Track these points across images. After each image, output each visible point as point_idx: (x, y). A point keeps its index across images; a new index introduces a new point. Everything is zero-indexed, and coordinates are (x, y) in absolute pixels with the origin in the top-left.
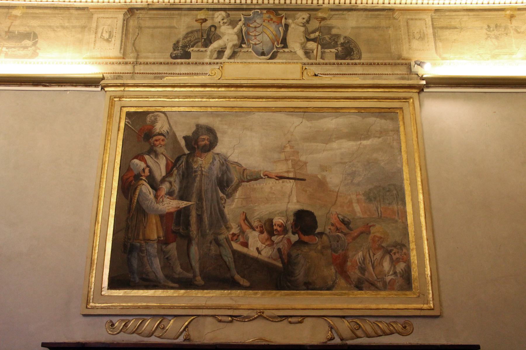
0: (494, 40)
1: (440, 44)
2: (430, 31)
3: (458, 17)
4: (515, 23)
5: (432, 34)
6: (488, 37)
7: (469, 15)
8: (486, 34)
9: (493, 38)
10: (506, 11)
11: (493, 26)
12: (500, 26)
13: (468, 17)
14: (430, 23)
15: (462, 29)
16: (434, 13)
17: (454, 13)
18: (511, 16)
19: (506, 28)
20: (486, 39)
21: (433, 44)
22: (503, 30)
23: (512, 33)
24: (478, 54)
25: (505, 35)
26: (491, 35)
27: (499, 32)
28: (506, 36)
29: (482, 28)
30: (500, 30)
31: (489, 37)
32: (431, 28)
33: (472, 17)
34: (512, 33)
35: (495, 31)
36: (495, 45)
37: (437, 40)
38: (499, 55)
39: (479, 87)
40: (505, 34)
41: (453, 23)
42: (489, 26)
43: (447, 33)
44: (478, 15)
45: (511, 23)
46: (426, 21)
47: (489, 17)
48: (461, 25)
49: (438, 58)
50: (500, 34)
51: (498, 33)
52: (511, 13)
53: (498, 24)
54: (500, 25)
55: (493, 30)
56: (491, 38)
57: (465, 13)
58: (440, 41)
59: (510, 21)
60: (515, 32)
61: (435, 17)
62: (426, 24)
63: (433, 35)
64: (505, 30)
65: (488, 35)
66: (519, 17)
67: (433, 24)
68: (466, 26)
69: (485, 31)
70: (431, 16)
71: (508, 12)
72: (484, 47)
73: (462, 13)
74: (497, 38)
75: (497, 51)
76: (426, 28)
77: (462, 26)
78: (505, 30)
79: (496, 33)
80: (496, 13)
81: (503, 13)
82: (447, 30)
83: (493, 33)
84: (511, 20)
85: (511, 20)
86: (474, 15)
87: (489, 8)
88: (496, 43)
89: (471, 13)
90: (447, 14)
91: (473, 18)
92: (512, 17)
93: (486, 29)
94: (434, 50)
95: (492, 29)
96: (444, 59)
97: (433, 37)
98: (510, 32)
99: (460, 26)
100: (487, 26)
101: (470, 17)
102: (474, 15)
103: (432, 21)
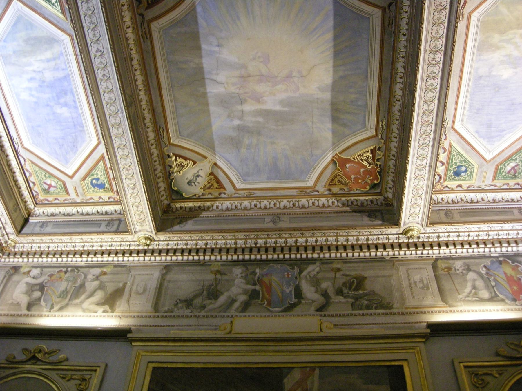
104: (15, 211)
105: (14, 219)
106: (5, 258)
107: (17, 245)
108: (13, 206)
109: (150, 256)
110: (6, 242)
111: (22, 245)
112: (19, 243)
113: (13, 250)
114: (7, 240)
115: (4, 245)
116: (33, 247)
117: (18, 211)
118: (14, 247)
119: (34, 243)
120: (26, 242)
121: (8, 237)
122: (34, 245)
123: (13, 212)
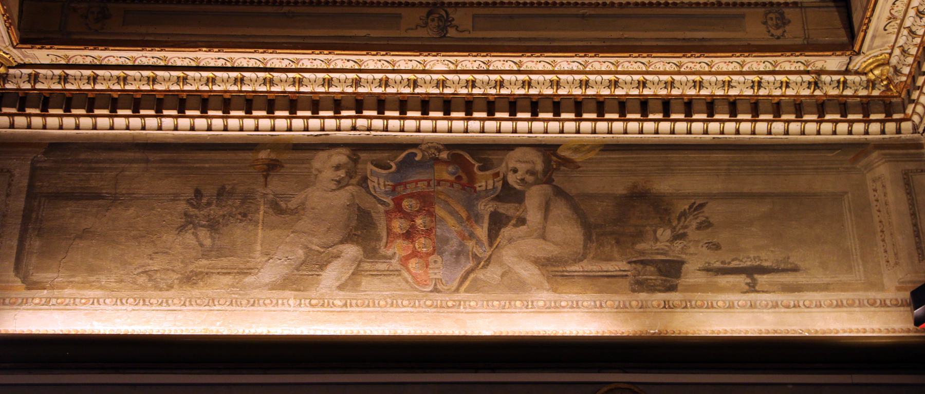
0: (203, 233)
1: (36, 243)
2: (19, 204)
3: (115, 166)
4: (276, 185)
5: (22, 213)
6: (188, 223)
7: (147, 161)
8: (186, 214)
9: (203, 226)
10: (258, 151)
11: (210, 190)
12: (231, 193)
13: (143, 165)
14: (25, 182)
15: (115, 199)
16: (44, 154)
17: (104, 155)
18: (268, 165)
19: (247, 198)
20: (182, 229)
21: (15, 243)
22: (238, 202)
23: (262, 213)
24: (143, 272)
25: (240, 217)
26: (197, 217)
27: (226, 209)
28: (241, 221)
29: (176, 198)
30: (230, 203)
31: (191, 223)
32: (24, 196)
33: (154, 165)
34: (262, 213)
35: (213, 207)
36: (201, 245)
37: (30, 231)
38: (207, 274)
39: (117, 370)
40: (240, 214)
41: (93, 184)
42: (198, 193)
43: (68, 210)
44: (175, 161)
45: (266, 185)
46: (12, 175)
47: (207, 165)
48: (116, 188)
49: (18, 283)
50: (224, 216)
51: (221, 213)
52: (273, 156)
53: (228, 188)
54: (233, 188)
55: (209, 204)
56: (195, 227)
57: (138, 155)
58: (38, 235)
59: (262, 180)
60: (271, 211)
61: (47, 165)
62: (10, 185)
63: (23, 216)
64: (243, 203)
65: (191, 216)
66: (292, 168)
67: (31, 186)
68: (130, 192)
69: (182, 206)
70: (33, 162)
71: (263, 155)
72: (166, 253)
73: (130, 155)
74: (213, 226)
75: (204, 262)
76: (8, 195)
77: (118, 191)
78: (243, 203)
79: (214, 210)
80: (229, 155)
81: (249, 155)
82: (70, 203)
83: (205, 212)
84: (266, 177)
85: (266, 177)
86: (163, 161)
87: (187, 141)
88: (208, 242)
89: (153, 156)
90: (83, 156)
91: (156, 168)
92: (272, 167)
93: (188, 200)
94: (13, 260)
95: (204, 201)
96: (32, 285)
97: (20, 221)
98: (257, 211)
99: (113, 192)
100: (192, 191)
101: (150, 165)
102: (163, 161)
103: (32, 177)
104: (783, 22)
105: (799, 41)
106: (914, 111)
107: (894, 61)
108: (765, 23)
109: (308, 118)
110: (872, 84)
111: (897, 52)
112: (890, 54)
113: (904, 79)
114: (864, 78)
115: (876, 93)
116: (914, 29)
117: (789, 13)
118: (897, 71)
119: (903, 21)
120: (894, 37)
121: (857, 73)
122: (908, 23)
123: (779, 32)
